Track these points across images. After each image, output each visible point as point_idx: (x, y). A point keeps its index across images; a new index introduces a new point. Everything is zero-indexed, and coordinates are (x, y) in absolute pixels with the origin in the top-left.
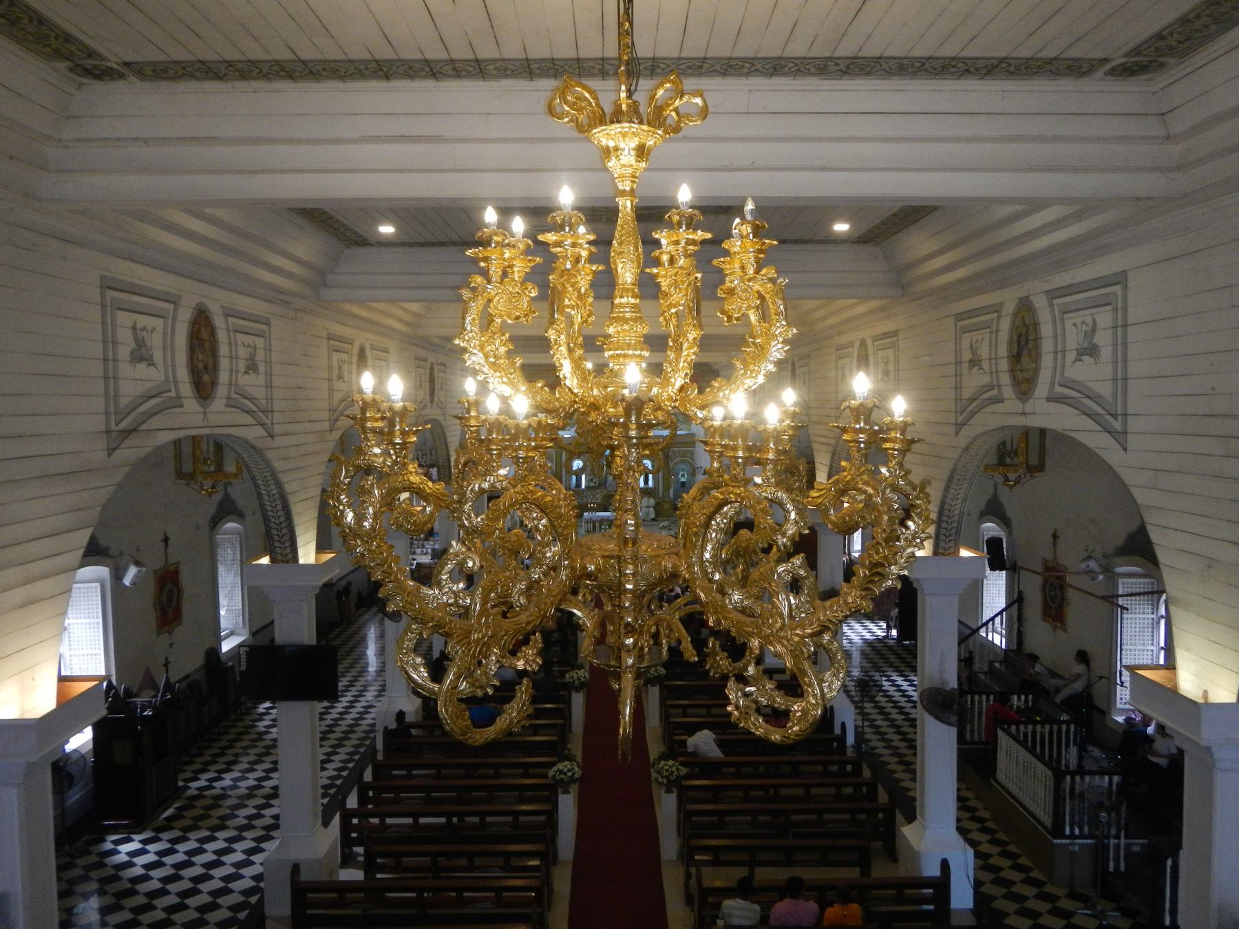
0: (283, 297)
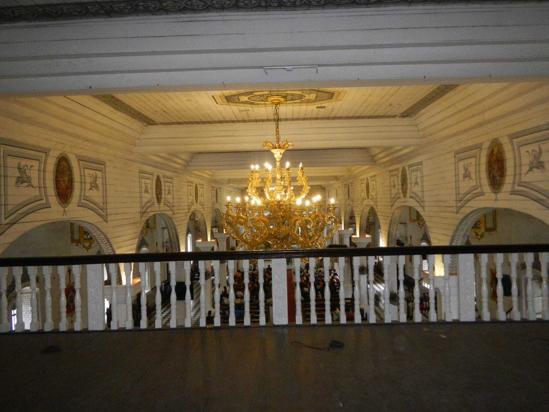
0: (176, 170)
